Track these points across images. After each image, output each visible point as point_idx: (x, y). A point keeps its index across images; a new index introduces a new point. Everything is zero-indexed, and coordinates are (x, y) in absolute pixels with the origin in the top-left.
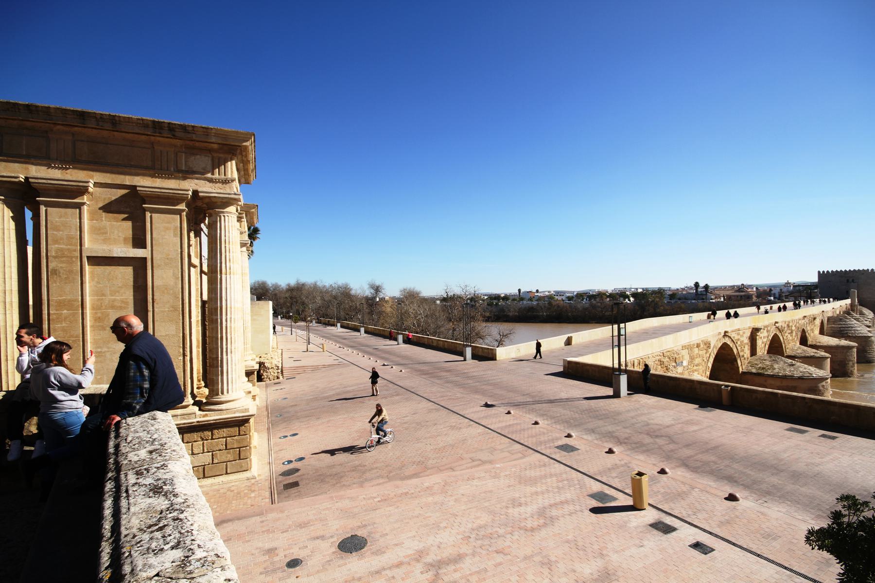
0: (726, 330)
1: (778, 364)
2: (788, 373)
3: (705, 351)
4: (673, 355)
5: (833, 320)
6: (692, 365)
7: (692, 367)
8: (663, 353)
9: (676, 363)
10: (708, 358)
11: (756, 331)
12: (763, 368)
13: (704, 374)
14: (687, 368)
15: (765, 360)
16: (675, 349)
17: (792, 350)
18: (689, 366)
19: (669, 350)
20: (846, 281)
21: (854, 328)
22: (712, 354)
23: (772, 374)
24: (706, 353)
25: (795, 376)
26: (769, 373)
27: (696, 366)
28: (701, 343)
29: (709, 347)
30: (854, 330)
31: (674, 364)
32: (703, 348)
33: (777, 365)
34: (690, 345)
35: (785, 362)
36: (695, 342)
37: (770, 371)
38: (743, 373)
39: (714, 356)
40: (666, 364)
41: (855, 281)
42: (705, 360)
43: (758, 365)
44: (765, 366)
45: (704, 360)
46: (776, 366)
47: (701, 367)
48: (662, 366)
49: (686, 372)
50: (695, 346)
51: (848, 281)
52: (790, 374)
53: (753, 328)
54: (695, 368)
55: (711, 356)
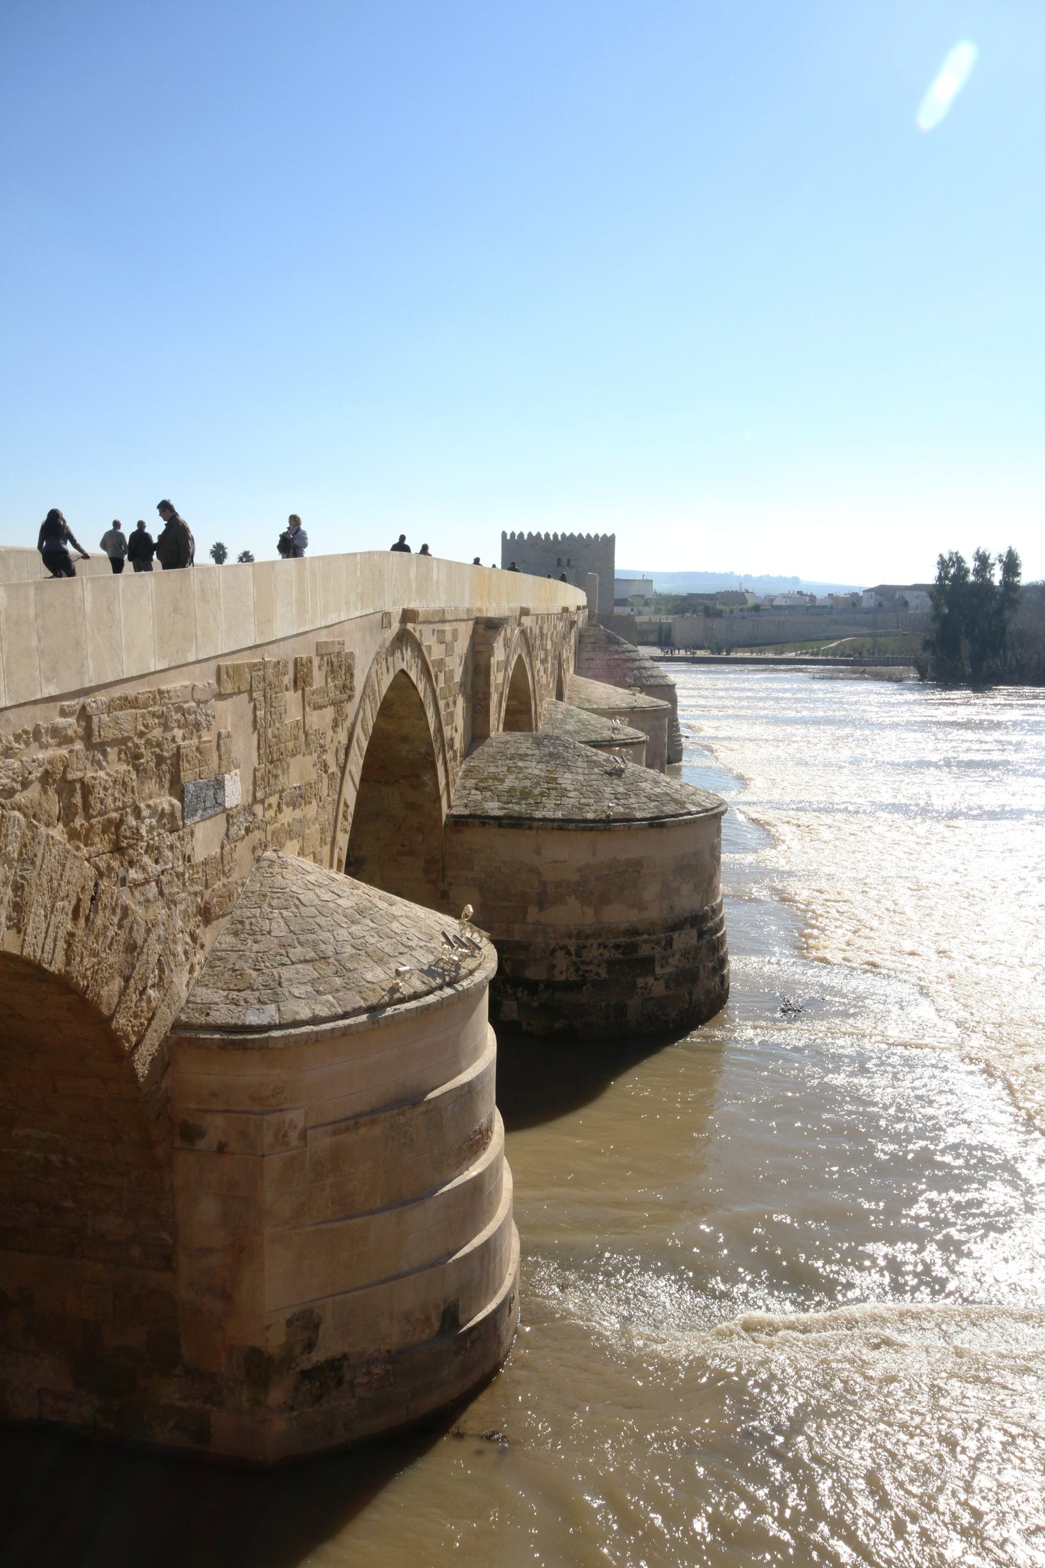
0: (413, 605)
1: (569, 768)
2: (614, 808)
3: (329, 712)
4: (157, 733)
5: (592, 640)
6: (274, 800)
7: (271, 813)
8: (84, 715)
9: (177, 789)
10: (342, 757)
11: (489, 633)
12: (525, 794)
13: (327, 849)
14: (242, 821)
15: (523, 757)
16: (176, 684)
17: (551, 720)
18: (258, 809)
19: (130, 690)
20: (555, 563)
21: (637, 663)
22: (358, 730)
23: (559, 815)
24: (335, 724)
25: (639, 815)
26: (549, 814)
27: (294, 805)
28: (316, 661)
29: (347, 688)
30: (638, 669)
31: (166, 801)
32: (324, 691)
33: (568, 775)
34: (264, 665)
35: (592, 763)
36: (288, 652)
37: (550, 803)
38: (458, 822)
39: (365, 745)
40: (109, 802)
41: (572, 563)
42: (333, 768)
43: (502, 781)
44: (528, 783)
45: (325, 767)
46: (566, 780)
47: (311, 810)
48: (79, 822)
49: (242, 851)
50: (288, 679)
51: (559, 560)
52: (621, 809)
53: (478, 621)
54: (288, 815)
55: (354, 744)
